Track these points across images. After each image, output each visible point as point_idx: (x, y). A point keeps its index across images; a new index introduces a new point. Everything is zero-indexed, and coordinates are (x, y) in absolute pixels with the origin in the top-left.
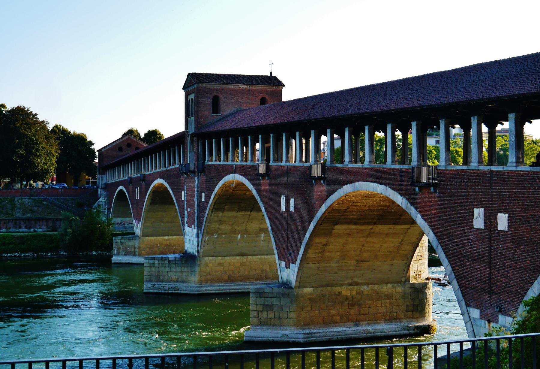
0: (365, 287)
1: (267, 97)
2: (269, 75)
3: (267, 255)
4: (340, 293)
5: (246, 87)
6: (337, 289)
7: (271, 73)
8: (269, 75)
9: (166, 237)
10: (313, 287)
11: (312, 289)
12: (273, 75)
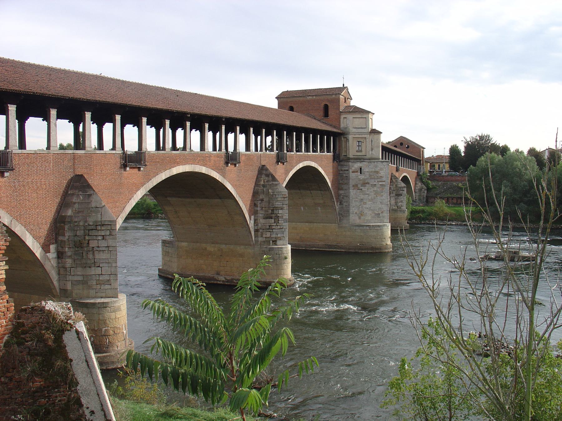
0: (223, 246)
2: (342, 86)
3: (328, 223)
4: (206, 249)
6: (204, 245)
7: (343, 85)
8: (342, 86)
10: (187, 242)
11: (187, 243)
12: (345, 86)
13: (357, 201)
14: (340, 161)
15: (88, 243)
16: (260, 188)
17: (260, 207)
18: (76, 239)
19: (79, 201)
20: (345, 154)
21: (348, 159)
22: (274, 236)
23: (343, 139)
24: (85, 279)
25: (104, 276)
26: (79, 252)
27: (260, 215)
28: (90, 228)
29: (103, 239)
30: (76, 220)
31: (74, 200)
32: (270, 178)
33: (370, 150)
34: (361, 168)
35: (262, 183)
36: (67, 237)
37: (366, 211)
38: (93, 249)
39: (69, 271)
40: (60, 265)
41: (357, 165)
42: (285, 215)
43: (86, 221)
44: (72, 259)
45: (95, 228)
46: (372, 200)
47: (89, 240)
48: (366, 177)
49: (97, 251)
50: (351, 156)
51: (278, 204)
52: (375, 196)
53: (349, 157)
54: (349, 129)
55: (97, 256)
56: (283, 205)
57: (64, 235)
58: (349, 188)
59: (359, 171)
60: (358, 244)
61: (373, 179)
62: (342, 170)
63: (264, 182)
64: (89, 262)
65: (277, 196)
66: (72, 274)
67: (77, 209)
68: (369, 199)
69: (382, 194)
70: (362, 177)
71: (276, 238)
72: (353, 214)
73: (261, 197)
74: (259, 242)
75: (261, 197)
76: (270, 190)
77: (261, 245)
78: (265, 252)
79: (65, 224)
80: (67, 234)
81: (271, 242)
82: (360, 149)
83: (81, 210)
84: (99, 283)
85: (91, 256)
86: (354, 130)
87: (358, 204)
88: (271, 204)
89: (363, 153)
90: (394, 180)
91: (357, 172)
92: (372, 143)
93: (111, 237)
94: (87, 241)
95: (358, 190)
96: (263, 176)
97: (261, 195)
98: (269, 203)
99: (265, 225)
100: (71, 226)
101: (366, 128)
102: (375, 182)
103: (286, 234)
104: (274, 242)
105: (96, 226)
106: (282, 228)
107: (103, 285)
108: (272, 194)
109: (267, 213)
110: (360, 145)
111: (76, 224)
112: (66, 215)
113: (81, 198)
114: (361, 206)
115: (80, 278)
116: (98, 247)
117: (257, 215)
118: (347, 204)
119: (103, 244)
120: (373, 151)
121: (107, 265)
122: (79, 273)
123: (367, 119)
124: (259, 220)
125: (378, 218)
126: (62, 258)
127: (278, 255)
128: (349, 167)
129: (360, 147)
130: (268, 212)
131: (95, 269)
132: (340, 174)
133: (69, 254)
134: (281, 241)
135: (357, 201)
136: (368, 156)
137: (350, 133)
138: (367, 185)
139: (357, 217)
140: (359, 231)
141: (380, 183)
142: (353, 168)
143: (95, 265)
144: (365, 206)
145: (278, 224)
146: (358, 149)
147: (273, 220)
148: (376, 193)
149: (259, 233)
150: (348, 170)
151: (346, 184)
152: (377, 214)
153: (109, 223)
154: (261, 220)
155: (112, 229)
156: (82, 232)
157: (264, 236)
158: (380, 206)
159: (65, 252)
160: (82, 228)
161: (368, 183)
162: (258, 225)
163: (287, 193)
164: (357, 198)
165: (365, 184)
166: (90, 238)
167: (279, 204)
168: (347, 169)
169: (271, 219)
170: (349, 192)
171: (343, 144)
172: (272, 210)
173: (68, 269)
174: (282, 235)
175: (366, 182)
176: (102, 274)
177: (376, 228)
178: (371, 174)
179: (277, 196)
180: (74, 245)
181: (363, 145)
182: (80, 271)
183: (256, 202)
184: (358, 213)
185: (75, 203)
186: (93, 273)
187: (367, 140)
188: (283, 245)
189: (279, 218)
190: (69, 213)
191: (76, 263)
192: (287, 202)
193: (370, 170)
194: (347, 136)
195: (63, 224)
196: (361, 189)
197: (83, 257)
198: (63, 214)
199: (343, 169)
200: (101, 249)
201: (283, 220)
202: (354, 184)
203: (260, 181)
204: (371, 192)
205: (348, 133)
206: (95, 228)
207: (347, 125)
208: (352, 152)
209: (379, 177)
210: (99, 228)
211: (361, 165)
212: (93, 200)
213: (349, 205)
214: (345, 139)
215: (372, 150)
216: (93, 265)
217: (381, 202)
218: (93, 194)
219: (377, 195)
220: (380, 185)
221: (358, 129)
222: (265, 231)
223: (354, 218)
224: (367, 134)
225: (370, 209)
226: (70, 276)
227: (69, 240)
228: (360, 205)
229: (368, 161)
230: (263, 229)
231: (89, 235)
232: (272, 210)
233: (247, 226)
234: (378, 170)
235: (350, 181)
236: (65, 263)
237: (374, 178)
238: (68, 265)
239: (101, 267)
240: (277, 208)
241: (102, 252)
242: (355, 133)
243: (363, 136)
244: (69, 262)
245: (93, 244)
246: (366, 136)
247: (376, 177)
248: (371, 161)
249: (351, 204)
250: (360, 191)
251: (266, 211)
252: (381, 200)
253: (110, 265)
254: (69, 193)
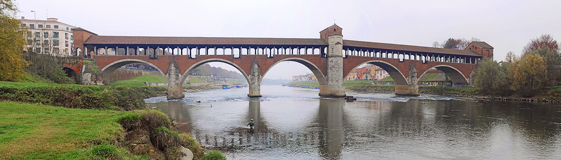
9: (401, 85)
34: (332, 60)
50: (330, 55)
70: (332, 64)
90: (412, 68)
138: (334, 68)
141: (338, 67)
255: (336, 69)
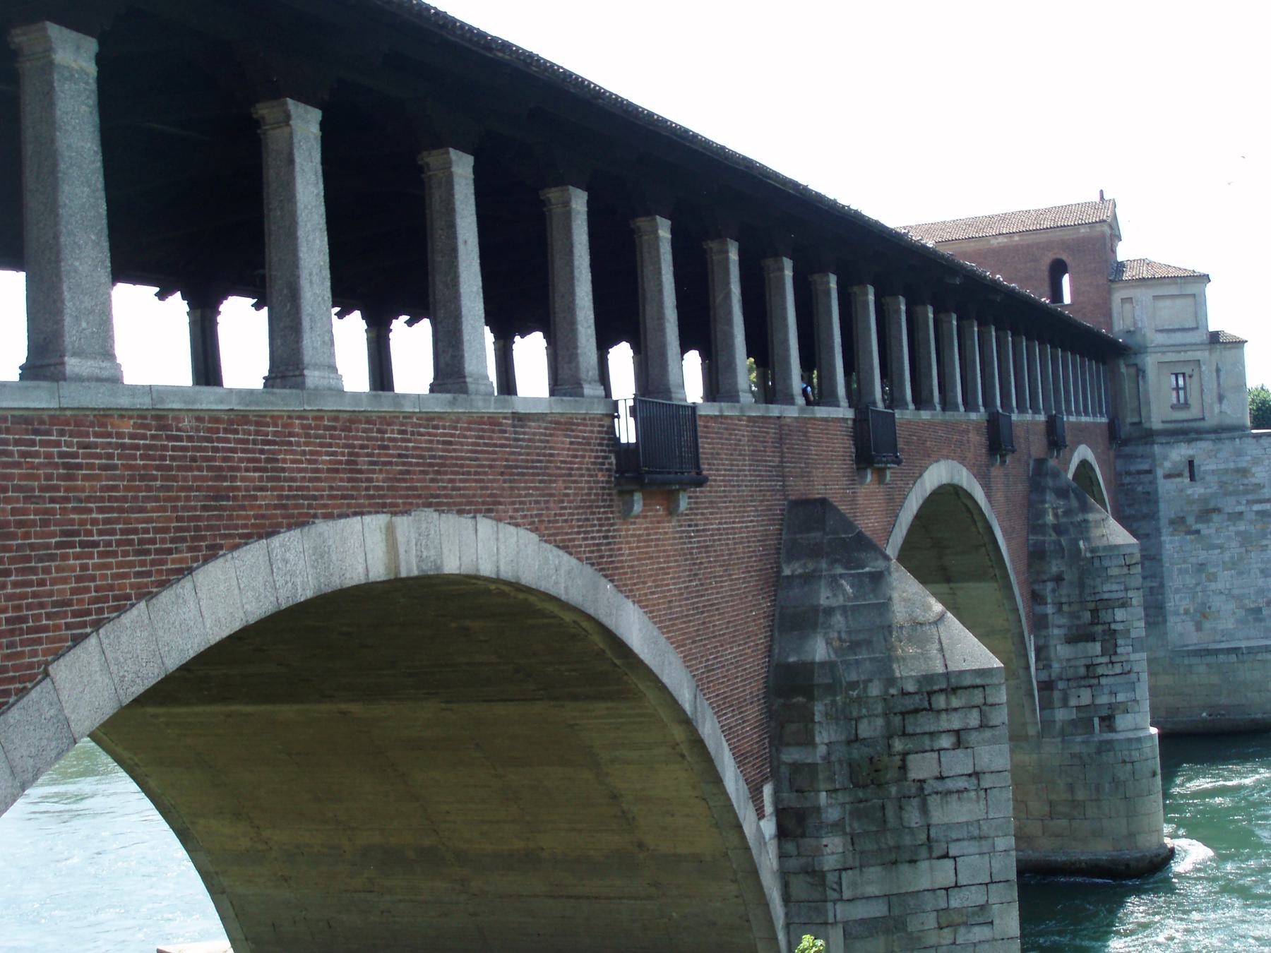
1: (1064, 258)
5: (1005, 240)
7: (1102, 192)
8: (1097, 199)
13: (1186, 571)
14: (1125, 442)
15: (903, 768)
16: (1047, 538)
17: (1054, 603)
18: (857, 753)
19: (841, 600)
20: (1136, 420)
21: (1149, 436)
22: (1104, 699)
23: (1123, 369)
24: (896, 912)
25: (964, 893)
26: (869, 804)
27: (1056, 631)
28: (910, 703)
29: (959, 744)
30: (853, 677)
31: (825, 598)
32: (1074, 503)
33: (1215, 399)
34: (1191, 463)
35: (1050, 518)
36: (822, 750)
37: (1217, 602)
38: (922, 789)
39: (835, 886)
40: (793, 863)
41: (1179, 453)
42: (1137, 624)
43: (891, 681)
44: (845, 834)
45: (926, 704)
46: (1234, 564)
47: (905, 755)
48: (1209, 491)
49: (937, 793)
50: (1156, 425)
51: (1110, 589)
52: (1243, 550)
53: (1151, 430)
54: (1144, 335)
55: (938, 815)
56: (1126, 590)
57: (808, 741)
58: (1158, 531)
59: (1187, 473)
60: (1204, 714)
61: (1231, 494)
62: (1128, 473)
63: (1056, 515)
64: (907, 840)
65: (1106, 563)
66: (847, 894)
67: (844, 636)
68: (1224, 563)
69: (1264, 542)
70: (1197, 490)
71: (1111, 706)
72: (1177, 614)
73: (1055, 567)
74: (1058, 726)
75: (1055, 567)
76: (1081, 543)
77: (1063, 734)
78: (1081, 758)
79: (811, 698)
80: (825, 736)
81: (1096, 721)
82: (1182, 400)
83: (861, 636)
84: (949, 920)
85: (913, 817)
86: (1161, 339)
87: (1190, 580)
88: (1087, 591)
89: (1194, 412)
91: (1180, 475)
92: (1218, 376)
93: (987, 734)
94: (898, 757)
95: (1189, 532)
96: (1050, 496)
97: (1054, 562)
98: (1082, 585)
99: (1072, 663)
100: (834, 702)
101: (1197, 328)
102: (1239, 503)
103: (1143, 692)
104: (1107, 723)
105: (930, 694)
106: (1129, 672)
107: (962, 930)
108: (1088, 555)
109: (1076, 622)
110: (1181, 382)
111: (855, 693)
112: (809, 659)
113: (848, 588)
114: (1199, 589)
115: (877, 910)
116: (941, 778)
117: (1044, 633)
118: (1154, 584)
119: (959, 763)
120: (1225, 402)
121: (971, 847)
122: (872, 890)
123: (1198, 301)
124: (1052, 649)
125: (1257, 624)
126: (803, 835)
127: (1129, 766)
128: (1154, 460)
129: (1181, 393)
130: (1079, 618)
131: (932, 869)
132: (1123, 485)
133: (833, 814)
134: (1129, 717)
135: (1186, 571)
136: (1211, 422)
137: (1149, 350)
138: (1215, 517)
139: (1192, 623)
140: (1203, 669)
141: (1257, 507)
142: (1167, 464)
143: (930, 849)
144: (1213, 586)
145: (1114, 659)
146: (1174, 401)
147: (1098, 646)
148: (1245, 539)
149: (1057, 695)
150: (1149, 472)
151: (1145, 517)
152: (1252, 609)
153: (978, 681)
154: (1059, 648)
155: (990, 700)
156: (880, 722)
157: (1073, 702)
158: (1260, 582)
159: (818, 810)
160: (879, 708)
161: (1218, 510)
162: (1050, 667)
163: (1136, 550)
164: (1185, 562)
165: (1207, 512)
166: (910, 746)
167: (1115, 587)
168: (1146, 467)
169: (1090, 645)
170: (1160, 545)
171: (1127, 386)
172: (1095, 612)
173: (831, 878)
174: (1130, 696)
175: (1211, 506)
176: (956, 886)
177: (1259, 657)
178: (1224, 479)
179: (1106, 563)
180: (851, 779)
181: (1194, 385)
182: (873, 881)
183: (1036, 587)
184: (1192, 611)
185: (829, 611)
186: (925, 883)
187: (1204, 368)
188: (1136, 729)
189: (1118, 636)
190: (819, 650)
191: (858, 848)
192: (1138, 581)
193: (1222, 466)
194: (1138, 361)
195: (801, 699)
196: (1198, 532)
197: (885, 822)
198: (792, 659)
199: (1133, 468)
200: (950, 785)
201: (1129, 642)
202: (1173, 516)
203: (1042, 513)
204: (1229, 538)
205: (1142, 350)
206: (926, 704)
207: (1135, 324)
208: (1159, 413)
209: (1250, 487)
210: (940, 701)
211: (1191, 452)
212: (895, 595)
213: (1162, 585)
214: (1132, 370)
215: (1221, 398)
216: (924, 852)
217: (1262, 571)
218: (888, 569)
219: (1250, 548)
220: (1258, 513)
221: (1173, 335)
222: (1072, 684)
223: (1180, 629)
224: (1203, 347)
225: (1229, 595)
226: (839, 906)
227: (833, 759)
228: (1197, 584)
229: (1213, 436)
230: (1068, 680)
231: (904, 734)
232: (1095, 612)
233: (1021, 672)
234: (1244, 465)
235: (1162, 506)
236: (818, 852)
237: (1236, 493)
238: (830, 862)
239: (954, 858)
240: (1109, 604)
241: (955, 796)
242: (1165, 348)
243: (1191, 355)
244: (833, 848)
245: (922, 767)
246: (1198, 355)
247: (1241, 487)
248: (1224, 435)
249: (1168, 583)
250: (1193, 537)
251: (1074, 615)
252: (1262, 561)
253: (985, 846)
254: (787, 572)
255: (1242, 527)
